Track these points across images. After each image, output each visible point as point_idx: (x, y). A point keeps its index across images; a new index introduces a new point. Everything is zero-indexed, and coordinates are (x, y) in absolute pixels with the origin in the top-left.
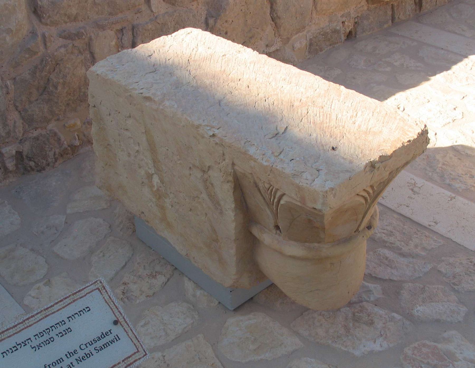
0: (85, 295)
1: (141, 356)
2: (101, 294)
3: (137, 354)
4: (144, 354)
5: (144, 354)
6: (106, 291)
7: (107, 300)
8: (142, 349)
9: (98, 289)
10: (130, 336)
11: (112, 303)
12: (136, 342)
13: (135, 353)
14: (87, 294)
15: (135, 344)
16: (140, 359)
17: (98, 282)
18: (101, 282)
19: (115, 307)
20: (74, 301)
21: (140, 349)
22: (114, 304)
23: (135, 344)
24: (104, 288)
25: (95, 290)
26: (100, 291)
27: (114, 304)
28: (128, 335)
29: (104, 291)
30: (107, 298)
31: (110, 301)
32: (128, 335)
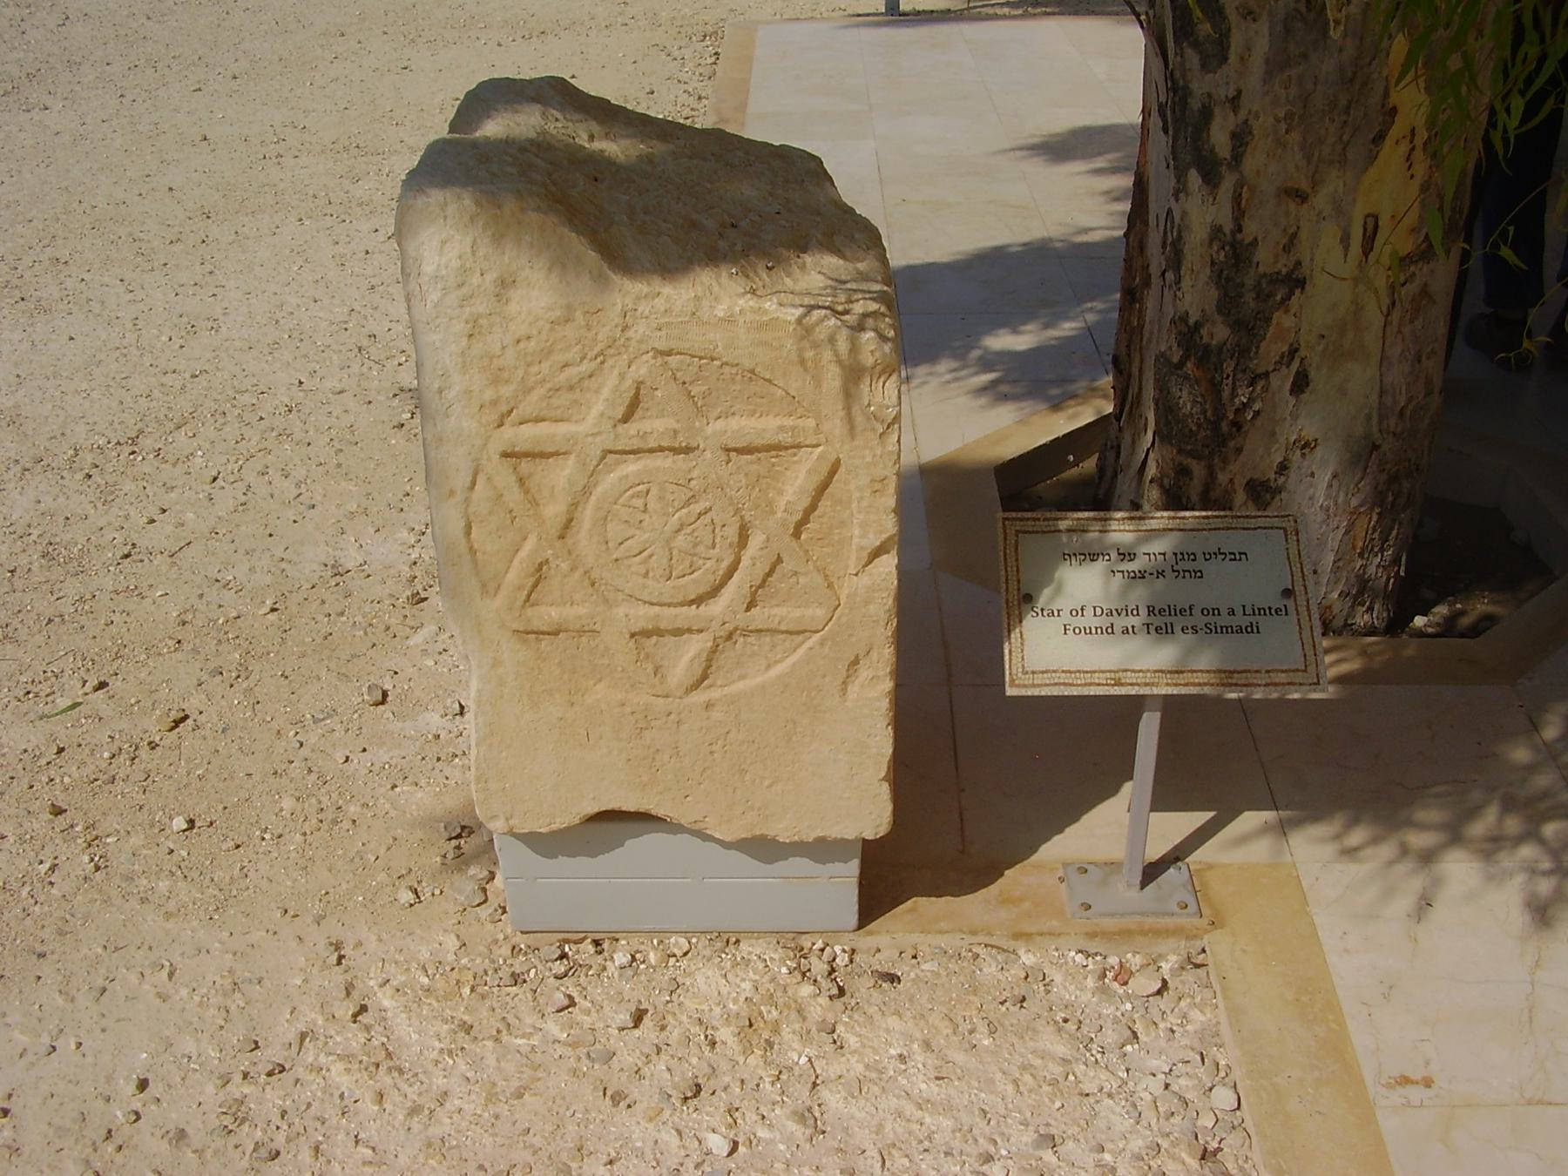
0: (1255, 529)
1: (1305, 681)
2: (1287, 540)
3: (1300, 673)
4: (1315, 680)
5: (1315, 680)
6: (1298, 541)
7: (1291, 556)
8: (1314, 670)
9: (1285, 530)
10: (1304, 636)
11: (1299, 565)
12: (1310, 653)
13: (1298, 670)
14: (1259, 527)
15: (1305, 656)
16: (1301, 684)
17: (1291, 518)
18: (1296, 521)
19: (1300, 574)
20: (1228, 529)
21: (1312, 668)
22: (1302, 568)
23: (1305, 656)
24: (1297, 534)
25: (1280, 528)
26: (1286, 535)
27: (1302, 568)
28: (1301, 634)
29: (1295, 538)
30: (1293, 552)
31: (1297, 559)
32: (1301, 634)
